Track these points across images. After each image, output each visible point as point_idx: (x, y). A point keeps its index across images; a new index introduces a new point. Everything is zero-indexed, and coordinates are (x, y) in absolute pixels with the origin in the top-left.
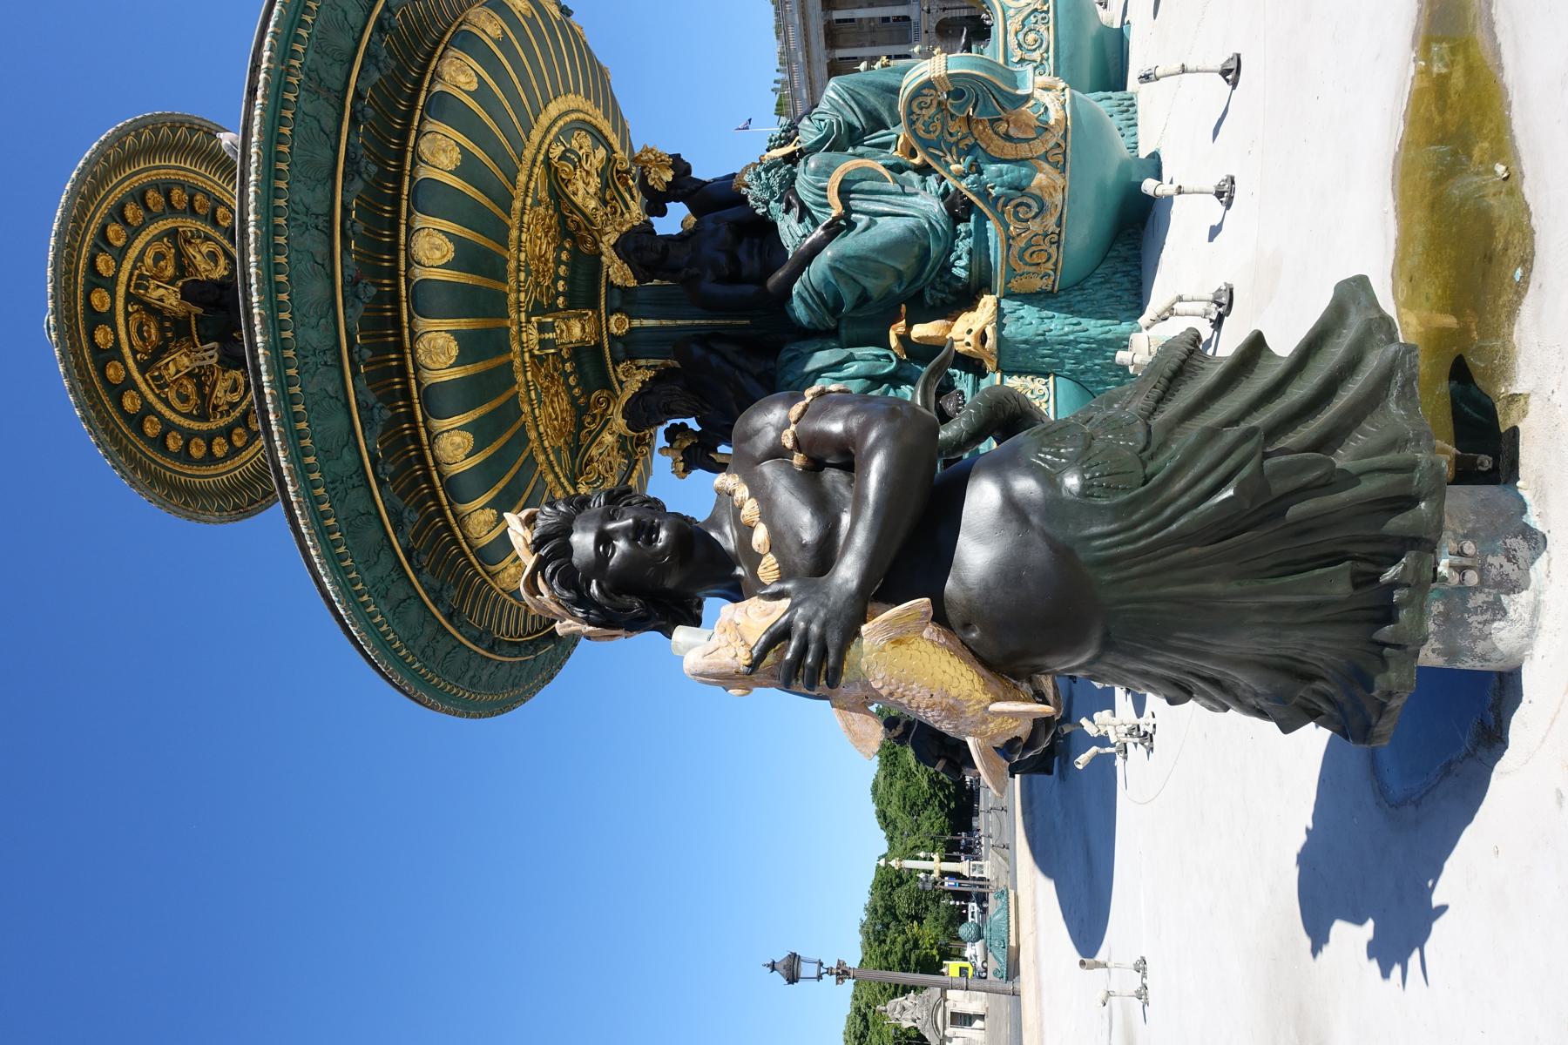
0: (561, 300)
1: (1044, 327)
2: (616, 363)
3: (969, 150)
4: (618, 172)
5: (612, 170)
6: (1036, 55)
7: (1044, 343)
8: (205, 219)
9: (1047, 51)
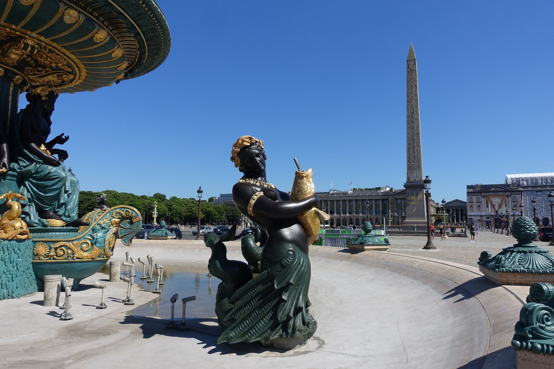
4: (62, 75)
6: (53, 253)
9: (54, 259)
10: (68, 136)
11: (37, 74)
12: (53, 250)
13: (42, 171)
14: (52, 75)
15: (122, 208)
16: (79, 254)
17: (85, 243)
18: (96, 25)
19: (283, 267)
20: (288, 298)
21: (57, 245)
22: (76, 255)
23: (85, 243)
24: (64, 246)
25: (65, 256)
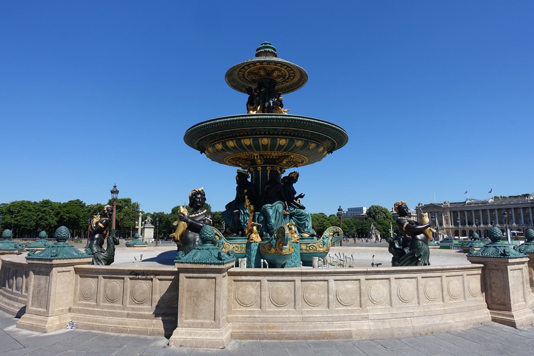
0: (265, 157)
1: (253, 250)
2: (253, 168)
3: (278, 237)
4: (297, 164)
5: (297, 163)
6: (308, 249)
7: (251, 250)
8: (288, 77)
9: (309, 251)
10: (304, 195)
11: (288, 166)
12: (308, 247)
13: (299, 212)
15: (334, 228)
16: (318, 249)
17: (320, 244)
18: (320, 146)
19: (418, 249)
20: (421, 260)
21: (310, 245)
22: (317, 250)
23: (320, 244)
25: (313, 250)
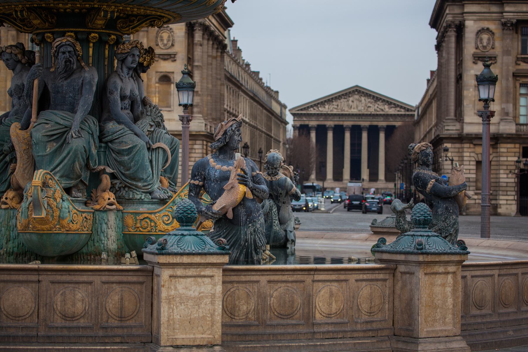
4: (154, 21)
12: (138, 221)
14: (145, 23)
21: (141, 217)
22: (158, 228)
24: (147, 218)
